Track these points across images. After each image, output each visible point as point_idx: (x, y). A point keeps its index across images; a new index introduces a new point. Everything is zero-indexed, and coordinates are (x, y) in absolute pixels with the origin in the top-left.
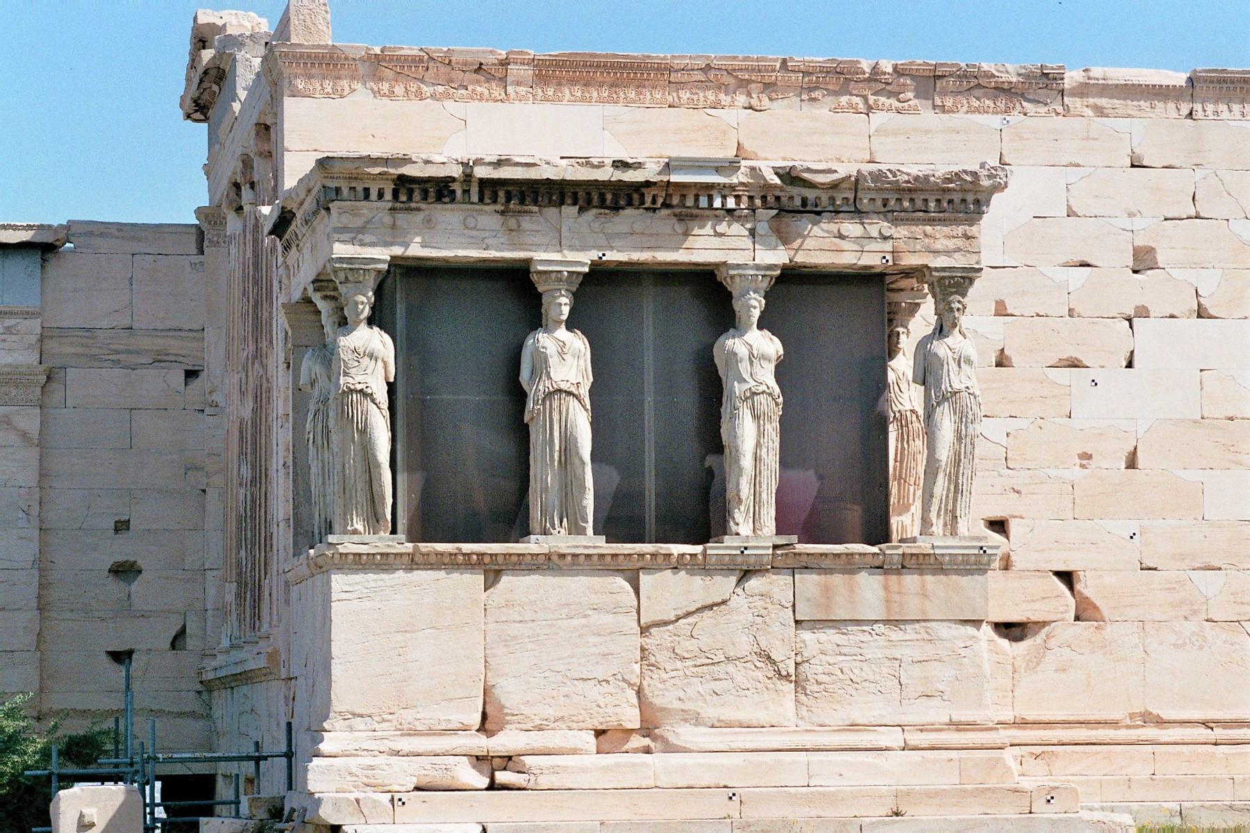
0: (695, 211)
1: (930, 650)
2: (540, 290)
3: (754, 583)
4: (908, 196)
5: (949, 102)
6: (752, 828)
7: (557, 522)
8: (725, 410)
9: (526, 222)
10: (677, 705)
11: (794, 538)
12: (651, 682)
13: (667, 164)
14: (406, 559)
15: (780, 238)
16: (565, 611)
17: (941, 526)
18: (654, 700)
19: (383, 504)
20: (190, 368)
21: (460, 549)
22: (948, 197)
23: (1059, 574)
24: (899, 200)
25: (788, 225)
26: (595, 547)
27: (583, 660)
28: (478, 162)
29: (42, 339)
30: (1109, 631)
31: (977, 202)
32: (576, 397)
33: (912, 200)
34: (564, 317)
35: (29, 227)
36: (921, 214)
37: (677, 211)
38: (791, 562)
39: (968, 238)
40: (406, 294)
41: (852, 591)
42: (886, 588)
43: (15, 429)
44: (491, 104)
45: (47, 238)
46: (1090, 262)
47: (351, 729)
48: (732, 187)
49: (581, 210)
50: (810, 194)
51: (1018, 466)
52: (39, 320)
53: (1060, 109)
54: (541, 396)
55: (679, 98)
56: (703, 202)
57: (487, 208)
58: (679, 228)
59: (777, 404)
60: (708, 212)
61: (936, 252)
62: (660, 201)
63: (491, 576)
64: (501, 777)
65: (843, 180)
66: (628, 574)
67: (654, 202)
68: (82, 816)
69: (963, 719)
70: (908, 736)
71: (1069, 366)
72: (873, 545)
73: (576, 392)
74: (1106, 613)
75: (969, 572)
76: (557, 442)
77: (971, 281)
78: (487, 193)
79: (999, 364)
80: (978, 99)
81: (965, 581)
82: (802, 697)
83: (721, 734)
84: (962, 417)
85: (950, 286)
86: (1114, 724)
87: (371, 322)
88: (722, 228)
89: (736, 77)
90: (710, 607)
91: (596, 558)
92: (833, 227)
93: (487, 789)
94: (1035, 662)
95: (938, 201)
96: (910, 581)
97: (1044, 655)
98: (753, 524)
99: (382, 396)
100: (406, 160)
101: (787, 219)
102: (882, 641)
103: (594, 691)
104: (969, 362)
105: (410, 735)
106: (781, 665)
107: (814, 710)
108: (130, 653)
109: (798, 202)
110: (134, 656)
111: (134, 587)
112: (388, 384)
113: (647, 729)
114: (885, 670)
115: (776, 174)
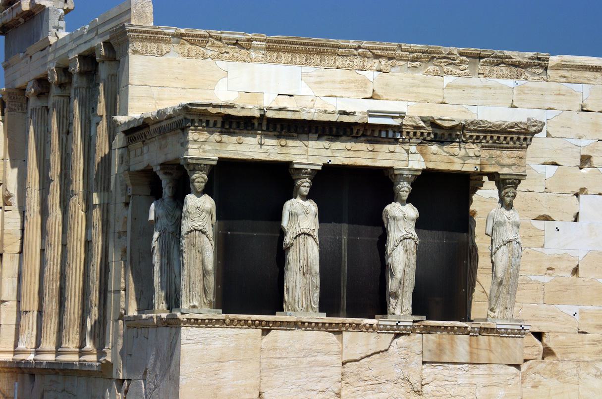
2: (294, 178)
11: (424, 317)
21: (250, 318)
25: (426, 148)
28: (269, 109)
37: (369, 138)
41: (452, 346)
42: (470, 345)
44: (240, 64)
56: (383, 134)
57: (270, 133)
60: (386, 140)
61: (502, 166)
65: (457, 125)
67: (357, 133)
73: (312, 235)
77: (519, 182)
78: (271, 125)
89: (373, 53)
90: (378, 353)
98: (401, 309)
102: (468, 375)
115: (424, 122)
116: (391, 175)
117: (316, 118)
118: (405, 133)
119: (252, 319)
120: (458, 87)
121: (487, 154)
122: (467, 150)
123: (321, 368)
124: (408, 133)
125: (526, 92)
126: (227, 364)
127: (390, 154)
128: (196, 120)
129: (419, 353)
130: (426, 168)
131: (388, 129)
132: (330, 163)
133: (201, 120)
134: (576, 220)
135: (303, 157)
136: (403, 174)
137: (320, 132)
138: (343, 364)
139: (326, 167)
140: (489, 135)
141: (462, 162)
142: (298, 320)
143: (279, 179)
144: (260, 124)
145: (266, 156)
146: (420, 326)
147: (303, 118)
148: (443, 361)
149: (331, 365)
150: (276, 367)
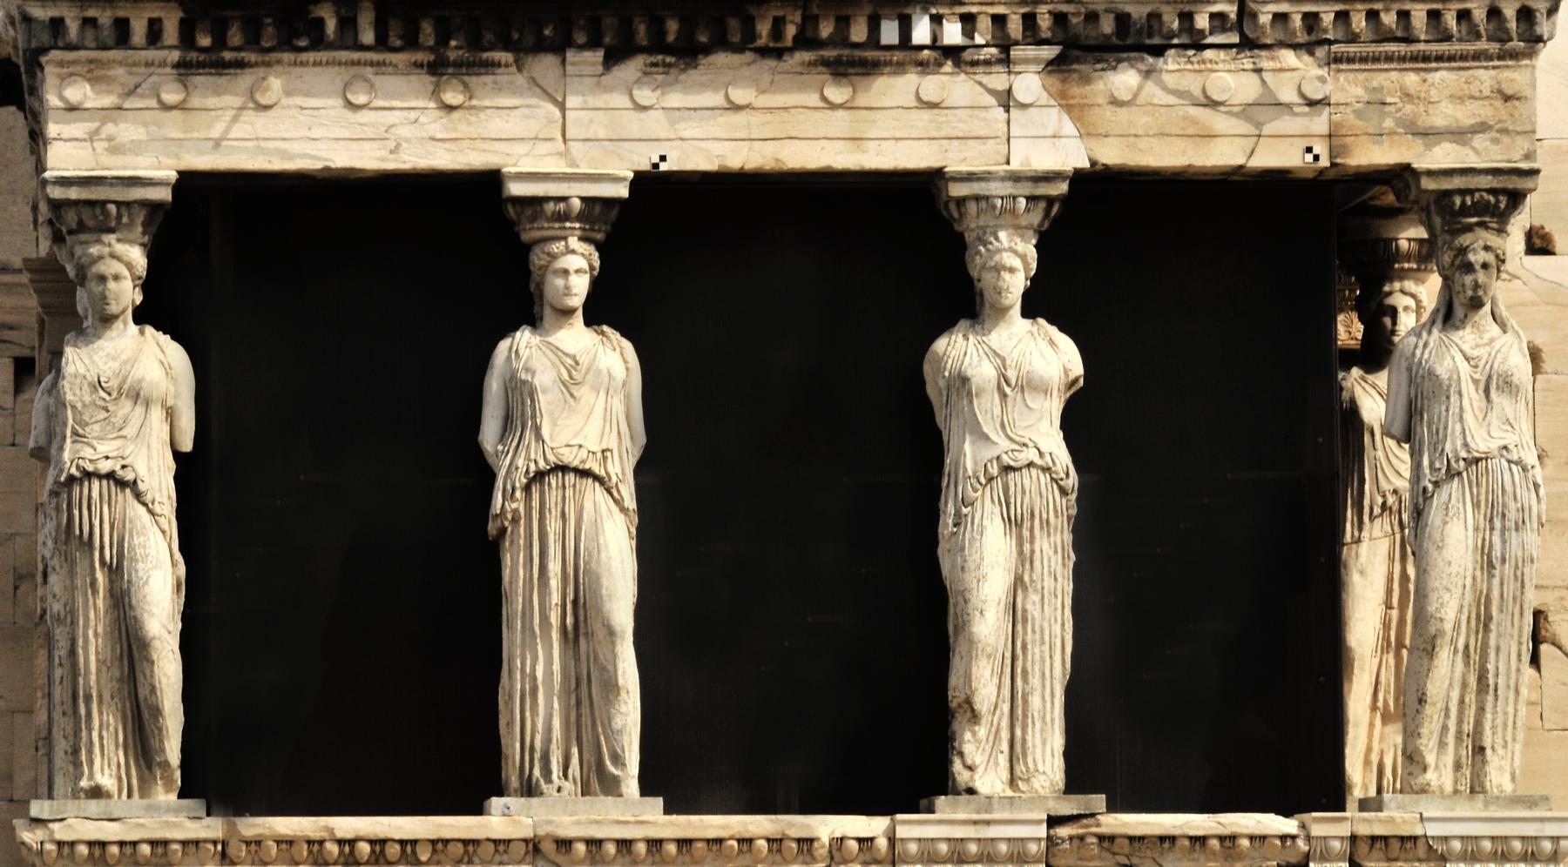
0: (870, 54)
21: (331, 831)
39: (1507, 98)
59: (1063, 492)
60: (897, 56)
61: (1429, 135)
62: (791, 31)
72: (1287, 813)
76: (554, 583)
84: (1495, 515)
88: (933, 85)
91: (641, 848)
109: (1107, 26)
116: (946, 204)
118: (984, 24)
119: (339, 835)
121: (1359, 91)
122: (1267, 76)
124: (999, 20)
127: (926, 115)
128: (68, 21)
130: (1087, 165)
131: (908, 11)
132: (663, 167)
133: (89, 22)
135: (543, 148)
136: (987, 198)
139: (648, 183)
140: (1359, 7)
141: (1245, 127)
142: (541, 832)
145: (379, 154)
146: (1082, 838)
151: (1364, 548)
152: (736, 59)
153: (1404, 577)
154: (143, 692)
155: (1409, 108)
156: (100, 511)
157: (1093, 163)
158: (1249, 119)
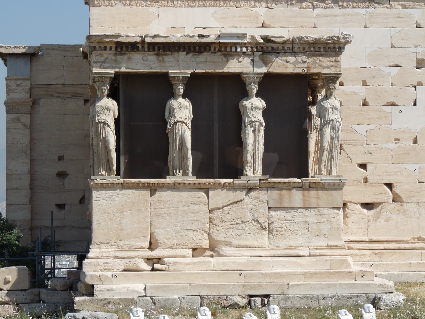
0: (230, 53)
1: (320, 219)
2: (173, 83)
3: (253, 194)
4: (312, 46)
5: (345, 4)
6: (247, 287)
7: (178, 171)
8: (243, 128)
9: (166, 58)
10: (223, 239)
12: (213, 231)
13: (219, 36)
14: (120, 185)
15: (264, 63)
16: (181, 204)
17: (325, 172)
18: (214, 237)
19: (112, 164)
20: (86, 99)
21: (140, 181)
22: (328, 46)
23: (387, 185)
24: (309, 48)
25: (266, 58)
26: (192, 180)
27: (187, 223)
28: (146, 36)
29: (31, 89)
30: (405, 206)
31: (340, 48)
32: (186, 124)
33: (314, 47)
34: (181, 94)
35: (25, 47)
36: (318, 53)
38: (267, 186)
39: (336, 61)
40: (118, 87)
41: (290, 196)
42: (303, 195)
43: (21, 122)
44: (168, 8)
45: (32, 51)
46: (400, 65)
47: (100, 248)
48: (245, 44)
49: (187, 53)
50: (275, 46)
51: (371, 143)
52: (29, 82)
53: (388, 6)
54: (172, 123)
55: (240, 4)
56: (234, 49)
57: (151, 53)
58: (225, 59)
59: (262, 126)
60: (235, 53)
61: (324, 67)
62: (217, 49)
63: (153, 191)
64: (156, 266)
65: (287, 40)
66: (205, 190)
67: (215, 49)
68: (5, 279)
69: (332, 244)
70: (311, 251)
71: (391, 105)
72: (299, 178)
74: (404, 199)
75: (336, 189)
76: (178, 141)
78: (151, 48)
79: (364, 104)
80: (356, 3)
81: (334, 193)
82: (271, 236)
83: (240, 250)
84: (334, 130)
85: (329, 80)
86: (407, 242)
87: (109, 96)
88: (241, 59)
90: (236, 202)
91: (192, 185)
92: (284, 58)
93: (151, 271)
94: (376, 218)
95: (324, 48)
96: (313, 193)
97: (380, 216)
98: (254, 171)
99: (112, 123)
100: (119, 36)
101: (267, 56)
103: (192, 234)
104: (336, 109)
105: (122, 251)
106: (263, 224)
107: (276, 241)
108: (64, 205)
109: (270, 49)
110: (66, 206)
111: (66, 180)
112: (115, 119)
113: (212, 248)
114: (303, 226)
115: (262, 38)
117: (182, 40)
119: (142, 182)
120: (324, 16)
123: (192, 215)
125: (375, 17)
126: (126, 213)
129: (265, 202)
132: (196, 71)
134: (415, 104)
137: (186, 50)
138: (211, 211)
142: (175, 182)
143: (163, 86)
144: (143, 47)
147: (172, 41)
148: (283, 206)
149: (201, 212)
150: (161, 214)
151: (312, 135)
152: (208, 53)
153: (319, 139)
154: (109, 158)
155: (320, 63)
156: (102, 128)
157: (267, 71)
158: (293, 64)
